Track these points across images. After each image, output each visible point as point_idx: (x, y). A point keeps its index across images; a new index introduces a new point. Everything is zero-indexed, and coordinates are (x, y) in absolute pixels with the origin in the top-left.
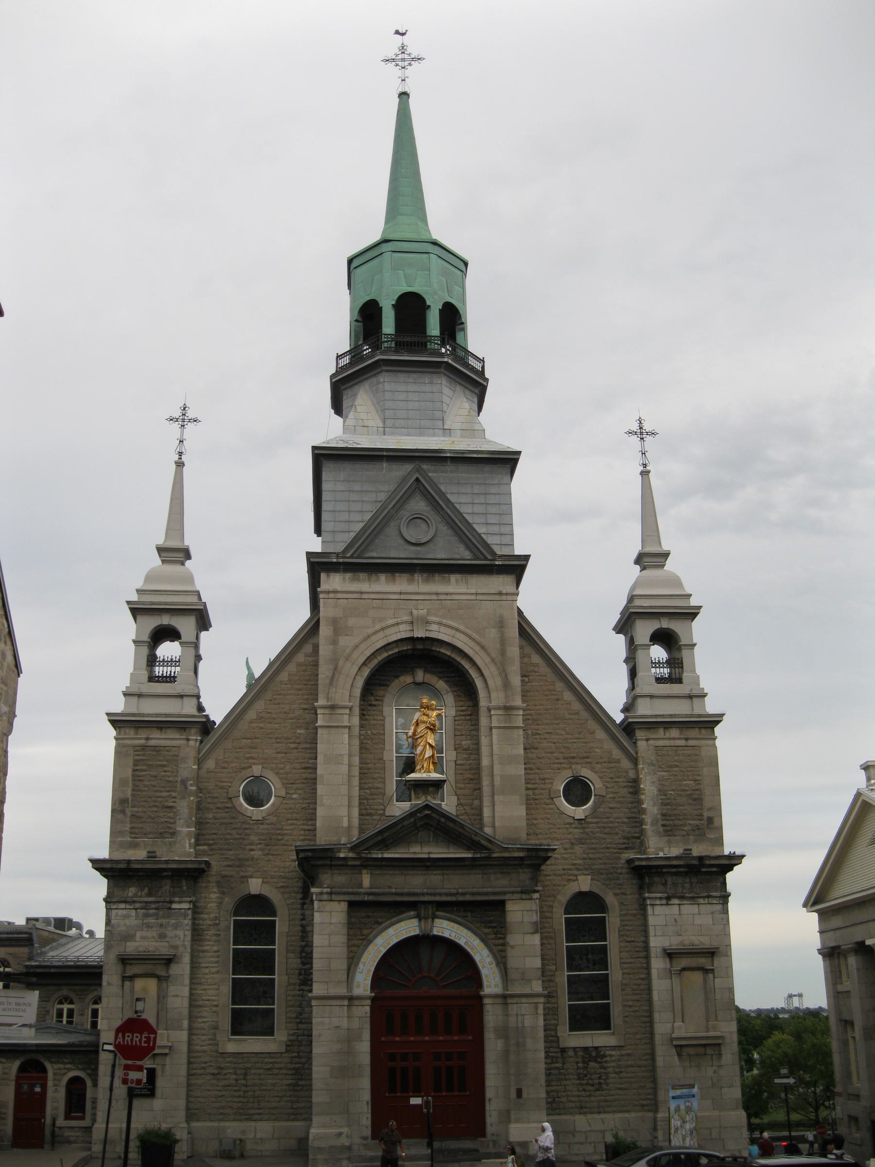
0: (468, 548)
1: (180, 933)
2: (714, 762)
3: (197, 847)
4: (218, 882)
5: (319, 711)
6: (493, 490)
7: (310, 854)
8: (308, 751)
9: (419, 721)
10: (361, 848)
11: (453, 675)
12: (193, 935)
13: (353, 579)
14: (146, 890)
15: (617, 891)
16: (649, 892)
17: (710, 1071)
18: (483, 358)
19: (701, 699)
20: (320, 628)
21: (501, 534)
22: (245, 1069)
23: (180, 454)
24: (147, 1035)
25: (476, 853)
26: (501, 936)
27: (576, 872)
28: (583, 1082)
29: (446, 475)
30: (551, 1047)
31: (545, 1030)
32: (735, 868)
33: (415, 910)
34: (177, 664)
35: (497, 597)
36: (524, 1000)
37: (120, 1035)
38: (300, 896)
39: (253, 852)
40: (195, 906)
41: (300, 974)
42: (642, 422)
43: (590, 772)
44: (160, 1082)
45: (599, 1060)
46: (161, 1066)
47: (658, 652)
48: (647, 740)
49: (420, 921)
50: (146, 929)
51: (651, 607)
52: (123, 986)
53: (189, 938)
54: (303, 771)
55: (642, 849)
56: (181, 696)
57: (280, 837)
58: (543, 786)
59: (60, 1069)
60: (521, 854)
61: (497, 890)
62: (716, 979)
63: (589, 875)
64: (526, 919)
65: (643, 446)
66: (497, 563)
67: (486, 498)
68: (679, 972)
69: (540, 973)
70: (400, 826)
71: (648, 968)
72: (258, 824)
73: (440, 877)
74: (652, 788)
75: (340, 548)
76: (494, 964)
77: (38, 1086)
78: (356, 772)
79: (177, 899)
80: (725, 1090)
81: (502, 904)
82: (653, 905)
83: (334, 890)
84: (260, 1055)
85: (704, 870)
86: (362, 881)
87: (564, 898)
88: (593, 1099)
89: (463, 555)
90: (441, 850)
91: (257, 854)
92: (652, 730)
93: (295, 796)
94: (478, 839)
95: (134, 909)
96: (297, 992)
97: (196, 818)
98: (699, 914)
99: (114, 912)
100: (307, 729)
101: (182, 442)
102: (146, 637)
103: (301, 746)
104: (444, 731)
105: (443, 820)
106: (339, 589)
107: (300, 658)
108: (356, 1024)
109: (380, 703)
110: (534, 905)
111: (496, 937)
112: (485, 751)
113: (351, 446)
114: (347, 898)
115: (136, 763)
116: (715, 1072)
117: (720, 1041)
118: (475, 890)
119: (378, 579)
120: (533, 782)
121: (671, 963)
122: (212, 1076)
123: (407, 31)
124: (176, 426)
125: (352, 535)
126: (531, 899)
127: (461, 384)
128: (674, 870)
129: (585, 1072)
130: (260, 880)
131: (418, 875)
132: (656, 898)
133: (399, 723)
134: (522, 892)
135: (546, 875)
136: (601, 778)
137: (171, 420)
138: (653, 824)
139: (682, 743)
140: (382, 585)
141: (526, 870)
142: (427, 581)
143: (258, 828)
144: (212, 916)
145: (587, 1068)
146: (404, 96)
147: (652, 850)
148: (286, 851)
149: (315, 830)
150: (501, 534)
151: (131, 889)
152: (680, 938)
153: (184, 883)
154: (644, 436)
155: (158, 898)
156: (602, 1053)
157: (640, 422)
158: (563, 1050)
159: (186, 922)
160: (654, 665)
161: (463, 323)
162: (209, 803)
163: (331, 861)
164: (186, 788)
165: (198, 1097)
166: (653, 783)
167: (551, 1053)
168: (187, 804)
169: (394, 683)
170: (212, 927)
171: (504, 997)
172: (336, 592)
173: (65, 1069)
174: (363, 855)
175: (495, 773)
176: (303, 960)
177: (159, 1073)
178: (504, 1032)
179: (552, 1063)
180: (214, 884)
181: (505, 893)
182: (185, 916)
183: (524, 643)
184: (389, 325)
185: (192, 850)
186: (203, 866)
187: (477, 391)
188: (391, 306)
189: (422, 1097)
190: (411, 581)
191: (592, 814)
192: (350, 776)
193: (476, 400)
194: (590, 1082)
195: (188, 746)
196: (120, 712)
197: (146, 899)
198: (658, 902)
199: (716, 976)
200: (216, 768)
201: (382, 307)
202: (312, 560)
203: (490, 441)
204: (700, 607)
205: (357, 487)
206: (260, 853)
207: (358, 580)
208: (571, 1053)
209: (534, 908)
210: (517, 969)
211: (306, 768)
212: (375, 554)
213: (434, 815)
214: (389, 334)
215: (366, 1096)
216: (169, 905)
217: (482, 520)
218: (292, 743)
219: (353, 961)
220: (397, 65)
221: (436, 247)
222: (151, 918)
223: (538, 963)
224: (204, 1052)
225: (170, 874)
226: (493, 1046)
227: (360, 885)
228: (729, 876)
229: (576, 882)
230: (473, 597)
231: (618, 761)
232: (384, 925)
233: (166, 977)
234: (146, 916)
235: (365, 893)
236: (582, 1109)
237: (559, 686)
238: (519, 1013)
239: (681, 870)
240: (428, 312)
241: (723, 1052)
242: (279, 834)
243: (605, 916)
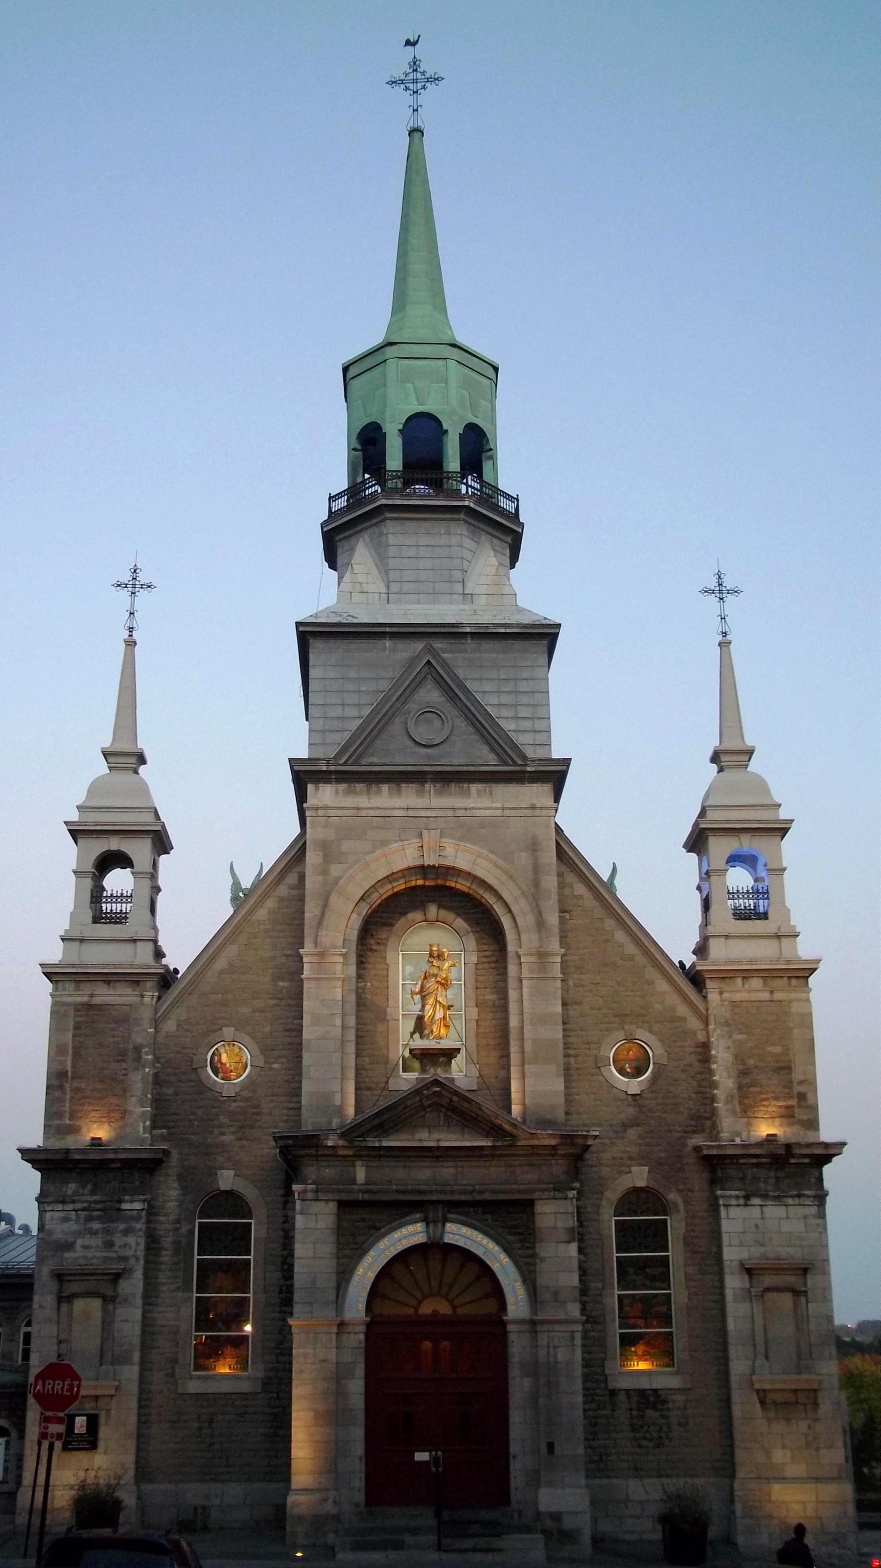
0: (493, 749)
1: (131, 1240)
2: (806, 1021)
3: (155, 1132)
4: (181, 1178)
5: (305, 960)
6: (526, 674)
7: (290, 1142)
9: (427, 974)
10: (354, 1135)
11: (472, 911)
12: (147, 1244)
13: (348, 792)
14: (89, 1187)
15: (681, 1187)
16: (722, 1189)
17: (803, 1425)
18: (518, 495)
19: (792, 939)
20: (307, 853)
21: (535, 731)
23: (131, 629)
24: (69, 1382)
25: (497, 1141)
26: (529, 1245)
27: (629, 1162)
28: (637, 1435)
29: (466, 656)
30: (598, 1389)
31: (584, 1366)
32: (835, 1159)
33: (421, 1212)
34: (129, 900)
35: (529, 812)
36: (557, 1327)
37: (40, 1382)
38: (281, 1192)
40: (151, 1206)
41: (281, 1291)
42: (722, 576)
43: (647, 1033)
44: (104, 1433)
45: (659, 1407)
48: (721, 993)
49: (427, 1224)
50: (88, 1236)
51: (728, 821)
52: (59, 1309)
54: (287, 1034)
55: (715, 1132)
56: (135, 941)
58: (588, 1051)
60: (554, 1142)
61: (524, 1187)
62: (809, 1304)
63: (645, 1165)
64: (560, 1225)
65: (722, 609)
66: (529, 769)
67: (516, 686)
68: (760, 1294)
69: (577, 1293)
70: (402, 1106)
71: (722, 1287)
73: (452, 1170)
74: (726, 1055)
75: (332, 752)
78: (351, 1036)
79: (127, 1198)
80: (822, 1452)
81: (531, 1203)
82: (727, 1206)
83: (320, 1186)
85: (792, 1161)
86: (355, 1175)
87: (613, 1195)
88: (650, 1457)
89: (488, 760)
90: (454, 1137)
91: (227, 1138)
92: (727, 981)
93: (276, 1066)
94: (499, 1122)
95: (74, 1210)
96: (277, 1315)
97: (152, 1094)
98: (787, 1218)
99: (48, 1215)
100: (291, 980)
101: (133, 614)
102: (89, 867)
103: (283, 1002)
104: (462, 983)
105: (455, 1099)
106: (331, 804)
107: (283, 890)
108: (347, 1357)
109: (382, 947)
110: (570, 1207)
111: (522, 1246)
112: (513, 1007)
113: (346, 622)
114: (337, 1196)
115: (77, 1027)
116: (809, 1427)
117: (815, 1386)
118: (497, 1187)
119: (379, 792)
120: (575, 1046)
121: (751, 1282)
123: (419, 37)
124: (125, 593)
125: (347, 735)
126: (566, 1198)
127: (487, 533)
128: (755, 1161)
129: (640, 1423)
130: (232, 1172)
132: (731, 1196)
133: (407, 972)
134: (555, 1190)
135: (592, 1166)
136: (660, 1040)
137: (119, 585)
138: (727, 1102)
141: (560, 1161)
142: (440, 793)
143: (230, 1106)
144: (172, 1218)
145: (643, 1417)
146: (416, 132)
147: (726, 1135)
149: (300, 1108)
150: (535, 731)
151: (70, 1185)
152: (762, 1249)
153: (136, 1176)
154: (724, 595)
155: (104, 1197)
156: (663, 1397)
157: (720, 577)
158: (613, 1393)
159: (139, 1226)
160: (731, 896)
161: (491, 450)
162: (168, 1075)
163: (317, 1150)
164: (140, 1057)
166: (728, 1048)
167: (597, 1395)
168: (140, 1077)
169: (400, 922)
171: (533, 1323)
172: (326, 808)
174: (356, 1143)
175: (525, 1037)
176: (284, 1273)
177: (102, 1420)
178: (533, 1368)
179: (599, 1408)
180: (175, 1178)
181: (534, 1191)
182: (137, 1219)
183: (564, 869)
184: (394, 461)
185: (147, 1135)
186: (160, 1156)
187: (509, 539)
188: (397, 432)
189: (430, 1451)
190: (421, 793)
191: (650, 1087)
192: (343, 1042)
193: (508, 552)
194: (648, 1435)
195: (143, 1004)
196: (57, 962)
197: (89, 1198)
198: (734, 1202)
199: (810, 1300)
200: (177, 1030)
201: (385, 433)
202: (296, 768)
203: (524, 610)
204: (792, 821)
205: (353, 674)
207: (355, 793)
208: (622, 1397)
209: (570, 1210)
210: (549, 1287)
212: (375, 760)
213: (444, 1092)
214: (394, 471)
216: (117, 1206)
217: (511, 714)
219: (344, 1275)
220: (407, 89)
221: (456, 350)
223: (574, 1279)
225: (119, 1165)
227: (354, 1181)
228: (827, 1169)
229: (629, 1175)
230: (499, 813)
231: (684, 1020)
232: (382, 1230)
233: (112, 1296)
234: (89, 1219)
235: (360, 1191)
236: (637, 1471)
237: (610, 923)
238: (551, 1344)
239: (764, 1160)
240: (445, 437)
241: (820, 1401)
242: (257, 1114)
243: (666, 1220)
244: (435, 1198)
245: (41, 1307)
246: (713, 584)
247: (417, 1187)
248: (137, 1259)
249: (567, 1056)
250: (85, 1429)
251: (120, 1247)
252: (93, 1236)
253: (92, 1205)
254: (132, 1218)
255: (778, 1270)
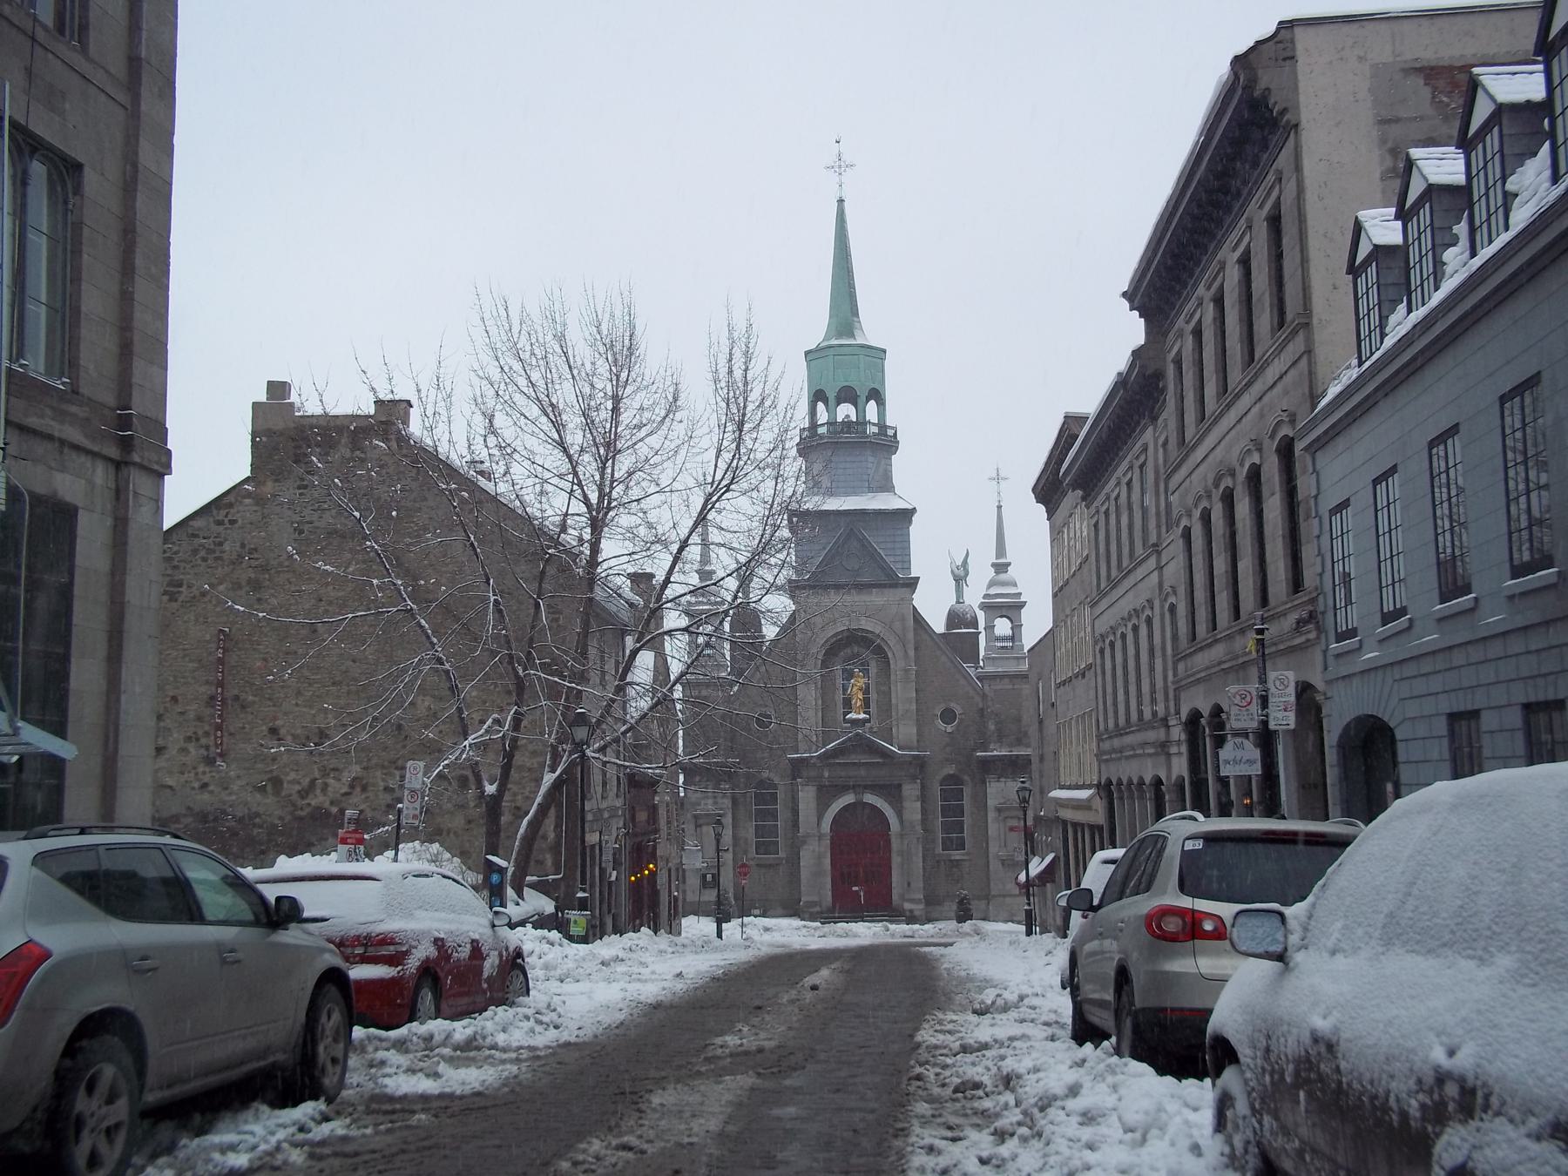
1: (726, 801)
6: (899, 532)
47: (1003, 627)
65: (999, 487)
87: (939, 777)
112: (893, 695)
139: (1011, 687)
140: (833, 598)
146: (841, 201)
158: (938, 862)
215: (829, 886)
219: (820, 817)
223: (919, 817)
226: (896, 860)
231: (973, 698)
246: (994, 475)
249: (917, 715)
255: (1008, 809)
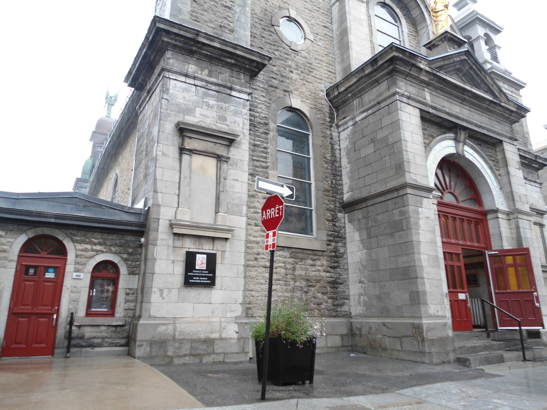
1: (240, 120)
8: (326, 16)
14: (206, 72)
22: (293, 264)
39: (292, 75)
46: (220, 252)
50: (206, 107)
52: (180, 160)
53: (247, 127)
57: (311, 70)
59: (86, 250)
72: (295, 54)
76: (498, 188)
77: (51, 270)
79: (238, 87)
84: (306, 252)
91: (294, 76)
95: (194, 85)
96: (332, 198)
103: (321, 11)
122: (264, 269)
131: (458, 105)
148: (316, 82)
165: (252, 290)
170: (262, 125)
173: (92, 250)
206: (297, 76)
211: (324, 27)
213: (469, 61)
216: (228, 91)
218: (314, 5)
222: (211, 98)
224: (258, 243)
234: (205, 95)
244: (465, 124)
245: (164, 154)
247: (458, 114)
248: (244, 135)
250: (205, 266)
251: (231, 122)
252: (210, 109)
253: (209, 85)
254: (240, 104)
